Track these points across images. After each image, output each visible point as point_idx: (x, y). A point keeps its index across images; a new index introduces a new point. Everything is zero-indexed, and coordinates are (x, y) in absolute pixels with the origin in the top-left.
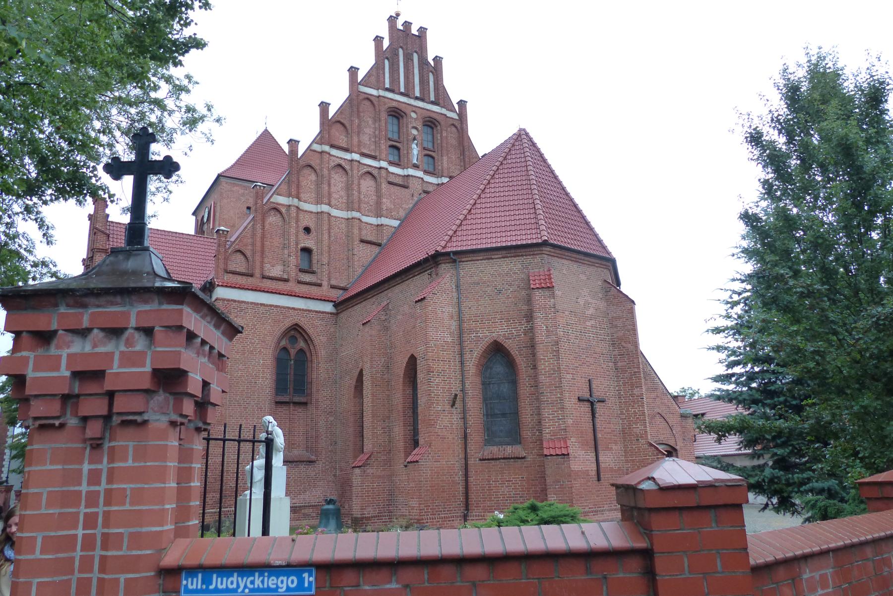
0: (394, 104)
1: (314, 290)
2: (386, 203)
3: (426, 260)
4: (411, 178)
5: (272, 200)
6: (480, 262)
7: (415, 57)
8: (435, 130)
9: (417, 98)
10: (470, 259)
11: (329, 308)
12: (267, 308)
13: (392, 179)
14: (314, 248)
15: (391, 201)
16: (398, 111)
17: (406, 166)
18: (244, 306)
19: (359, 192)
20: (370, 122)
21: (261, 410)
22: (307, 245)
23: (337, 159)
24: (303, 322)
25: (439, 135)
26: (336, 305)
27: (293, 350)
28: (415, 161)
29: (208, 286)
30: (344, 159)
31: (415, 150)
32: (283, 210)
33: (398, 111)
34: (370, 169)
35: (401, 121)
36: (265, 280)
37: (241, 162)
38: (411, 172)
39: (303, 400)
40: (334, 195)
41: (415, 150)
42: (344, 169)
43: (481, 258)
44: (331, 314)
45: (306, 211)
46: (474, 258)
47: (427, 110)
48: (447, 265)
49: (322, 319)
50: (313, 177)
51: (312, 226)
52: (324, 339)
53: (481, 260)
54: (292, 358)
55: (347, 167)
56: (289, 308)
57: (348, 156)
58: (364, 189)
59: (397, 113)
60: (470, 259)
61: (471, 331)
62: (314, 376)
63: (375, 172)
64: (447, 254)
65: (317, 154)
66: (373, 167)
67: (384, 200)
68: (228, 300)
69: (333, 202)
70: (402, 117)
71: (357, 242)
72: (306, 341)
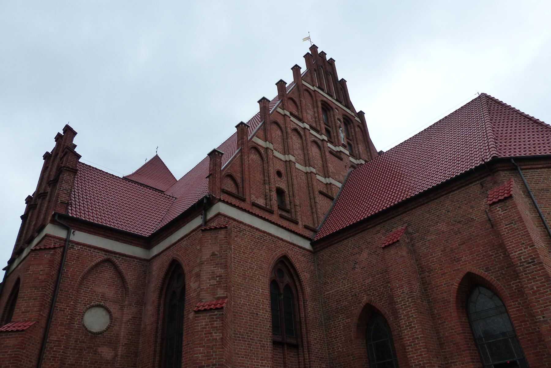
0: (325, 99)
1: (292, 227)
3: (478, 169)
4: (342, 154)
5: (253, 140)
6: (540, 170)
8: (349, 127)
10: (529, 167)
11: (307, 245)
12: (262, 234)
15: (333, 167)
16: (327, 105)
17: (337, 144)
20: (310, 107)
21: (264, 349)
22: (281, 187)
23: (295, 124)
24: (290, 255)
25: (353, 130)
26: (313, 244)
27: (281, 284)
28: (343, 142)
29: (205, 201)
30: (299, 126)
31: (342, 135)
32: (262, 151)
33: (327, 105)
34: (316, 139)
35: (328, 113)
36: (254, 207)
37: (138, 172)
38: (342, 149)
39: (294, 342)
42: (299, 133)
43: (541, 166)
45: (277, 158)
46: (534, 166)
47: (344, 110)
48: (506, 172)
49: (304, 255)
50: (279, 132)
51: (283, 171)
52: (307, 276)
53: (541, 168)
54: (282, 292)
55: (302, 133)
56: (278, 238)
57: (301, 124)
60: (529, 167)
63: (319, 142)
64: (507, 160)
65: (281, 115)
66: (318, 138)
67: (329, 165)
68: (229, 218)
70: (329, 110)
71: (317, 192)
72: (291, 276)
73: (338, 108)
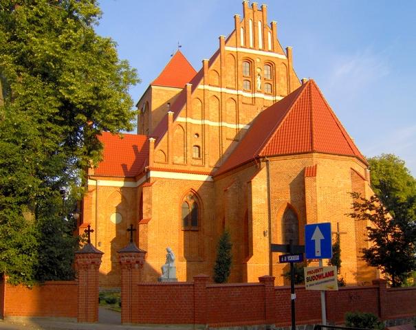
0: (246, 55)
2: (242, 115)
7: (260, 24)
9: (260, 50)
13: (244, 101)
14: (201, 146)
18: (164, 180)
19: (226, 110)
28: (259, 89)
39: (196, 229)
40: (212, 114)
41: (259, 82)
44: (211, 182)
55: (219, 97)
58: (228, 108)
59: (249, 61)
61: (275, 197)
62: (202, 216)
63: (235, 98)
69: (211, 118)
73: (259, 56)
